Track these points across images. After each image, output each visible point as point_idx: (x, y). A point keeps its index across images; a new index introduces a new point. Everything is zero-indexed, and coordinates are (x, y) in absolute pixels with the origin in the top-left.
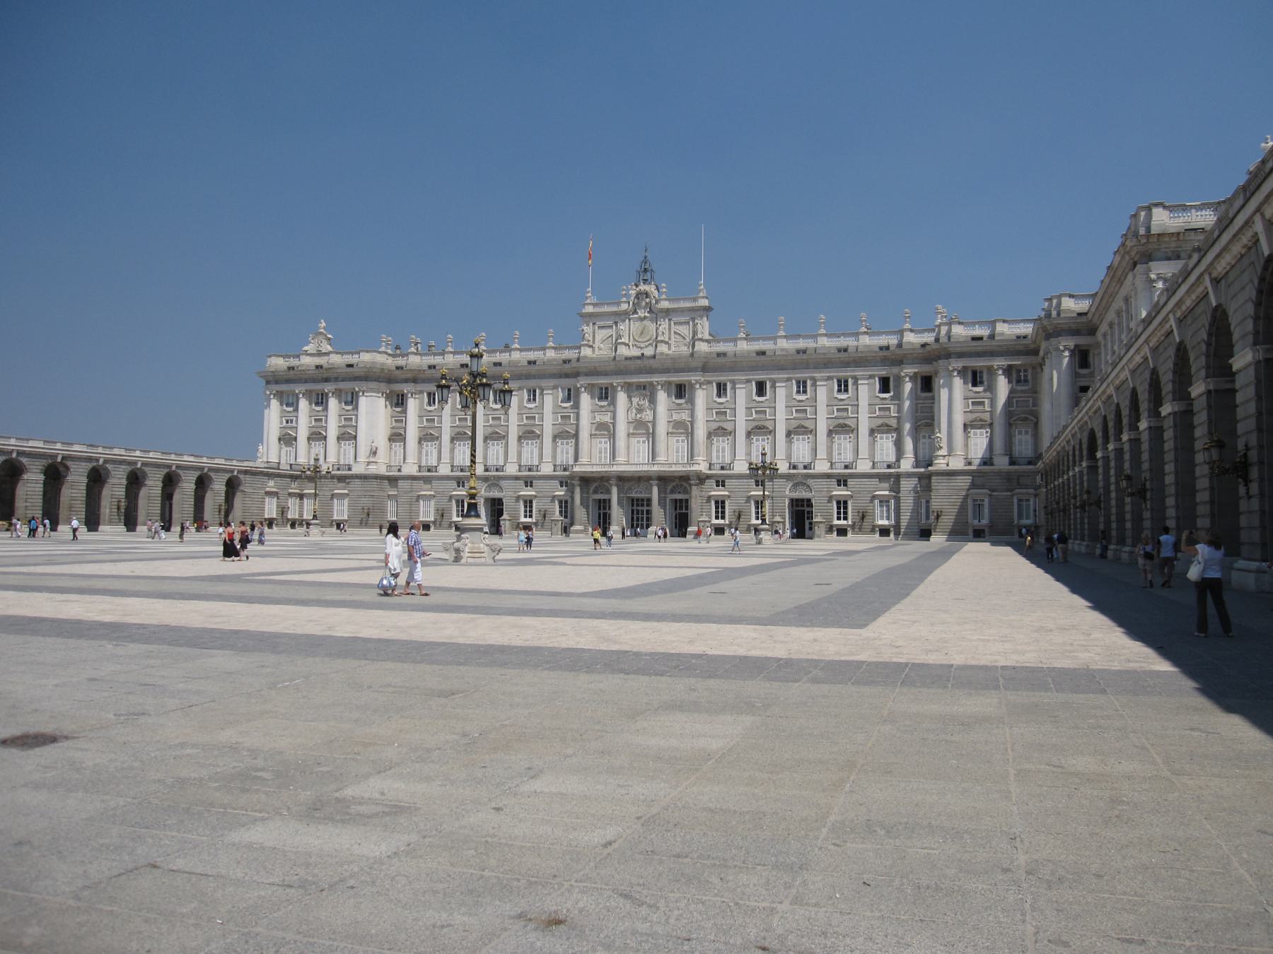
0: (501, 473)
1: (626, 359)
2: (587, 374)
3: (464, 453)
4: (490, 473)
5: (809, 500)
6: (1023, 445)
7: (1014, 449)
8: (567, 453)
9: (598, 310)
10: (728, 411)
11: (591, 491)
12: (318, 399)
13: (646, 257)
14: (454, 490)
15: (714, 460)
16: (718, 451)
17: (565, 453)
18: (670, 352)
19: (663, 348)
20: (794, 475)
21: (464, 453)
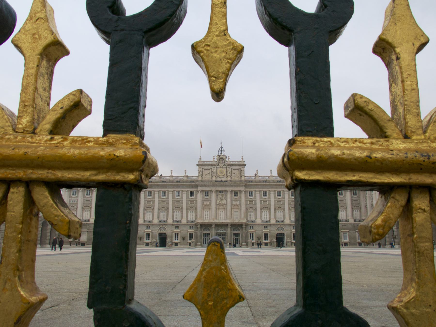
0: (167, 223)
1: (216, 181)
2: (201, 187)
3: (150, 215)
4: (162, 223)
5: (284, 233)
6: (357, 215)
7: (354, 216)
8: (192, 215)
9: (203, 163)
10: (253, 201)
11: (202, 230)
12: (88, 192)
13: (221, 146)
14: (146, 229)
15: (249, 219)
16: (250, 215)
17: (191, 216)
18: (232, 180)
19: (229, 178)
20: (278, 224)
21: (150, 215)
